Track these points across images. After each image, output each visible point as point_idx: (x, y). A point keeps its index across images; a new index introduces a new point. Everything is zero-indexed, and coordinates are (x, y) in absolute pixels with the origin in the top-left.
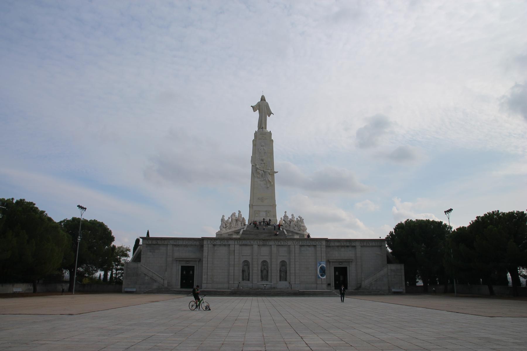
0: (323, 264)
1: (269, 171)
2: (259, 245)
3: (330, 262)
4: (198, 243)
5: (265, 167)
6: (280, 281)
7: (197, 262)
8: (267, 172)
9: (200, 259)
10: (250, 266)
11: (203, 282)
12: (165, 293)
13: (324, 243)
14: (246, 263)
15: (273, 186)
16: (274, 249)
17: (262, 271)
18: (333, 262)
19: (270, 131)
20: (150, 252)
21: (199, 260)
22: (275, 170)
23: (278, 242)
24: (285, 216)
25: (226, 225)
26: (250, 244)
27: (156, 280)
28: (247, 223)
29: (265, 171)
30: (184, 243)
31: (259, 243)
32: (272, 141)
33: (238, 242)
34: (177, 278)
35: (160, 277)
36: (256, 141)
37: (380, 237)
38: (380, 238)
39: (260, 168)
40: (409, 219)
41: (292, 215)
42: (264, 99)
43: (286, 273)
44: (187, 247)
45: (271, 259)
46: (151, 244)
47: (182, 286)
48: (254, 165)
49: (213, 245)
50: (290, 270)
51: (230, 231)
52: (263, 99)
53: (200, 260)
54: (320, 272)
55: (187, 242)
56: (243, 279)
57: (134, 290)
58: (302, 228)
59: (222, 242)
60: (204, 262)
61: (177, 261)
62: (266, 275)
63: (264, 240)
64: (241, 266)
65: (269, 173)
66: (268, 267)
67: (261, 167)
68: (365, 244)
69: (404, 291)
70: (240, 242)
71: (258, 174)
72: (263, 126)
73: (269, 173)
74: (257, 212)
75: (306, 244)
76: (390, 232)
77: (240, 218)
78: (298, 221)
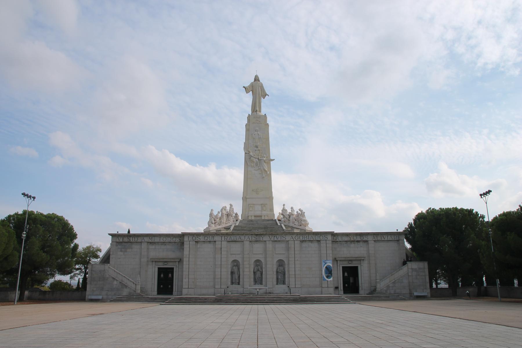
0: (329, 263)
1: (265, 159)
2: (250, 241)
3: (337, 261)
4: (177, 240)
5: (260, 155)
6: (277, 284)
7: (177, 263)
8: (262, 160)
9: (180, 259)
10: (241, 266)
11: (183, 287)
12: (136, 301)
13: (330, 237)
14: (236, 264)
15: (269, 176)
16: (270, 245)
17: (254, 273)
18: (340, 260)
19: (265, 114)
20: (121, 251)
21: (179, 260)
22: (272, 158)
23: (274, 237)
24: (284, 210)
25: (214, 220)
26: (240, 240)
27: (126, 284)
28: (240, 218)
29: (260, 158)
30: (162, 241)
31: (251, 239)
32: (268, 125)
33: (226, 238)
34: (153, 283)
35: (131, 281)
36: (249, 125)
37: (397, 230)
38: (396, 231)
40: (431, 208)
41: (292, 208)
42: (258, 79)
43: (284, 274)
44: (165, 245)
45: (266, 258)
46: (121, 242)
47: (160, 292)
48: (248, 152)
49: (195, 241)
50: (289, 271)
51: (220, 227)
52: (257, 79)
53: (181, 261)
54: (326, 273)
55: (165, 239)
56: (232, 283)
57: (100, 297)
58: (303, 222)
59: (206, 238)
60: (184, 263)
61: (153, 261)
62: (260, 278)
63: (257, 235)
64: (230, 266)
65: (264, 161)
66: (262, 268)
68: (379, 238)
69: (429, 295)
70: (229, 238)
71: (252, 163)
72: (258, 109)
73: (264, 161)
74: (252, 206)
75: (308, 240)
76: (409, 223)
77: (232, 212)
78: (298, 215)
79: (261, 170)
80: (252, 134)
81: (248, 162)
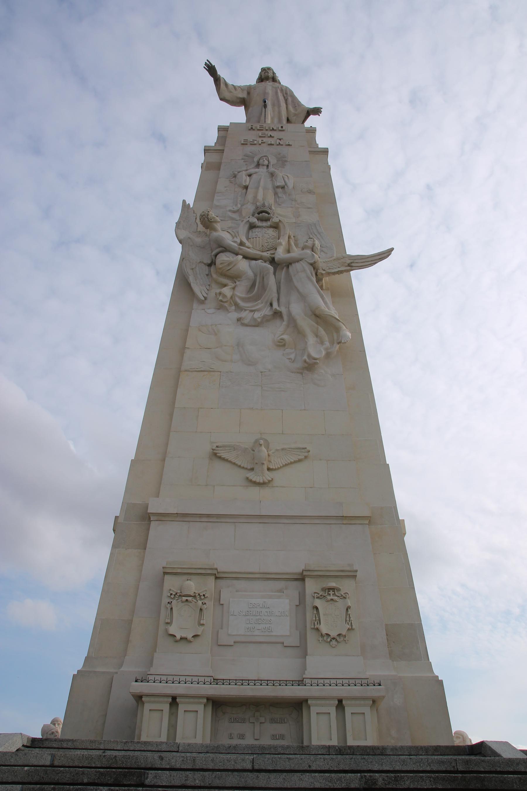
36: (222, 151)
39: (242, 244)
65: (313, 265)
67: (248, 244)
79: (293, 323)
80: (235, 176)
81: (191, 279)
